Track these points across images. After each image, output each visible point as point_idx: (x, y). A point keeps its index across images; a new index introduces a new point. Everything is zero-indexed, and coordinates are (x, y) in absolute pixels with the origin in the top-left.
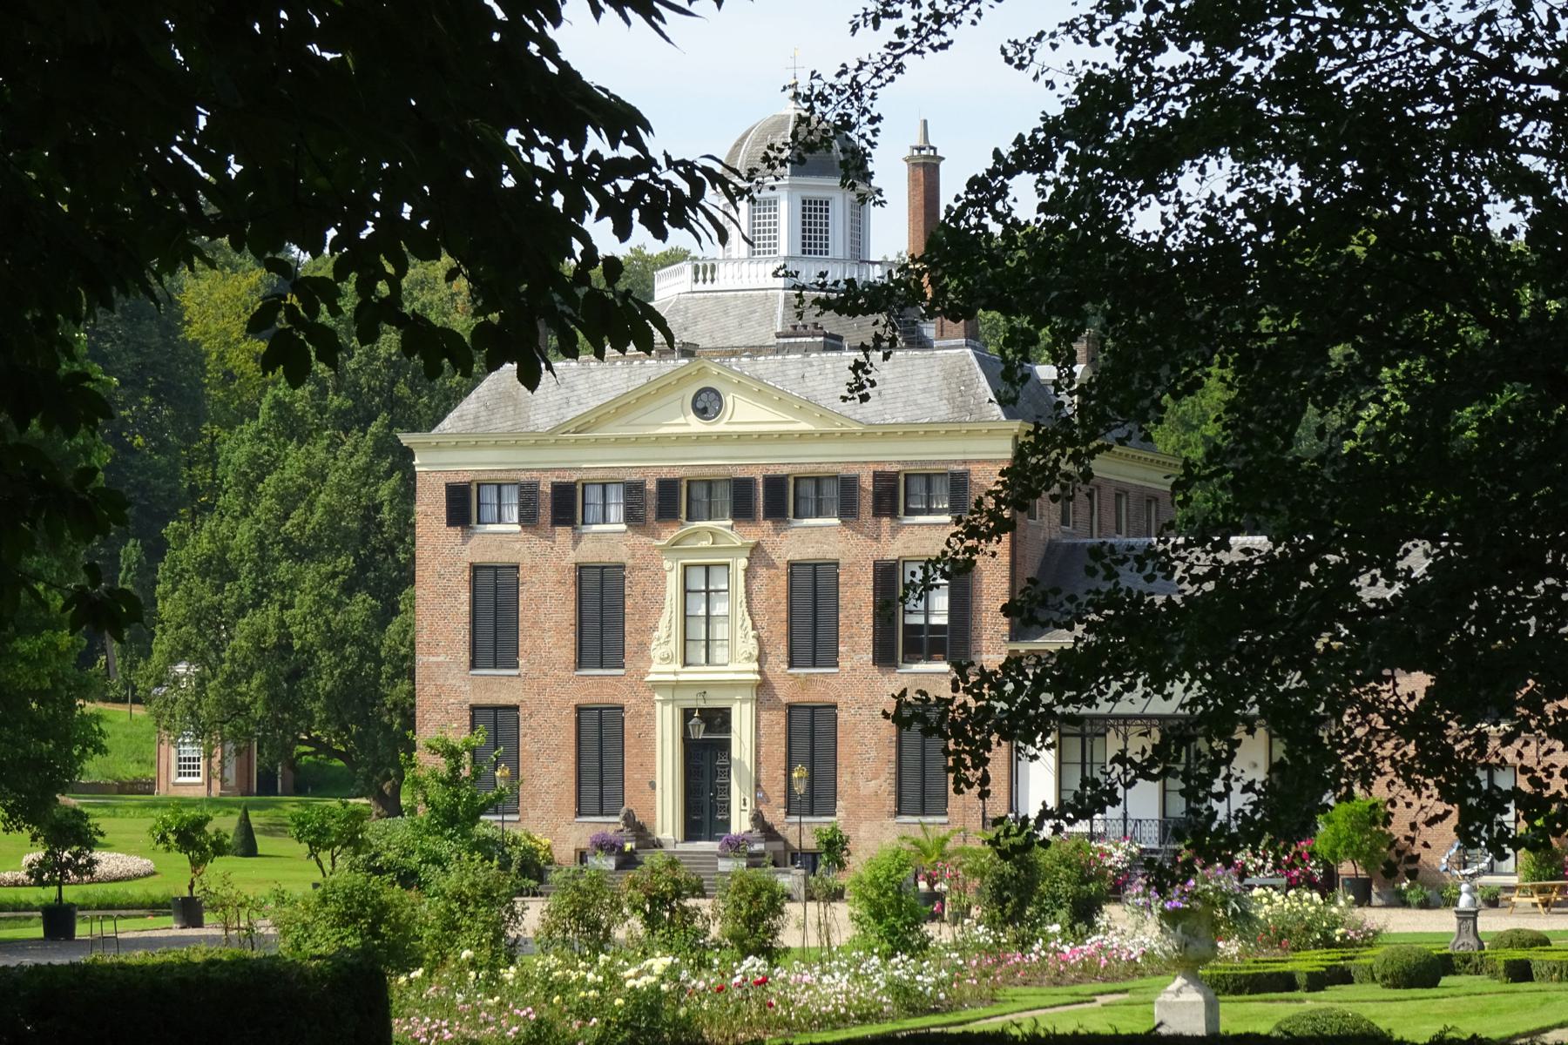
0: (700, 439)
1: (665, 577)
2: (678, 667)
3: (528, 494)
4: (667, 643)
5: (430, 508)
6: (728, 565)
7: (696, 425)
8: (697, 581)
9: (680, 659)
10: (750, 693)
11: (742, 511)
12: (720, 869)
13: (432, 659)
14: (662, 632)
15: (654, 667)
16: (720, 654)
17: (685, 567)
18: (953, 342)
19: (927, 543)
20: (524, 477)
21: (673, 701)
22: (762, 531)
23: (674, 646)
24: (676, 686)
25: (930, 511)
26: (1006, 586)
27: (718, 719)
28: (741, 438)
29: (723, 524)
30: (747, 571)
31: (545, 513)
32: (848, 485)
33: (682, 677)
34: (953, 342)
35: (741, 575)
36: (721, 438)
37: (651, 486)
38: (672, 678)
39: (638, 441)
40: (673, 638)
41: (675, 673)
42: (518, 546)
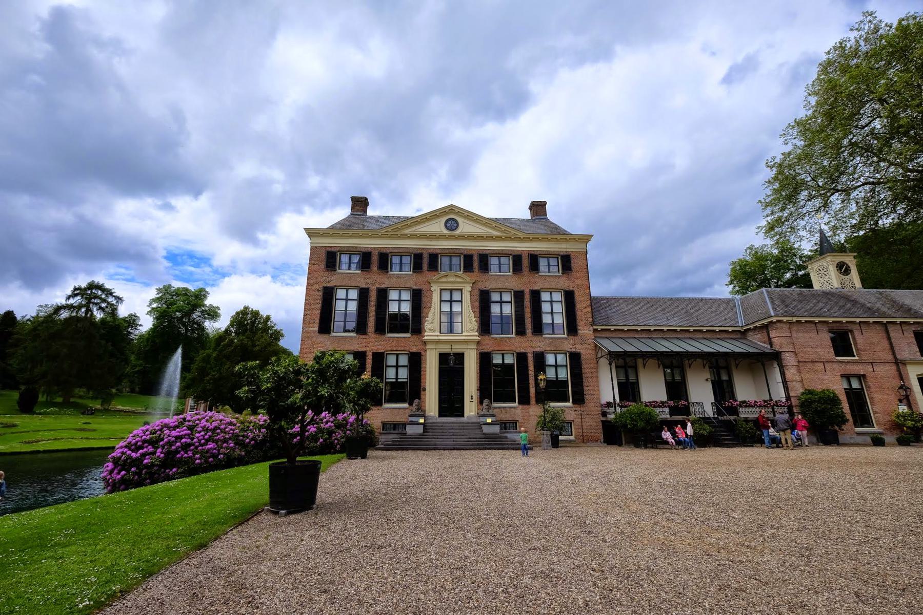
1: (431, 294)
2: (439, 334)
4: (432, 322)
6: (461, 290)
7: (446, 232)
8: (446, 296)
9: (438, 330)
11: (468, 266)
12: (484, 432)
13: (312, 329)
14: (429, 319)
15: (426, 334)
16: (457, 327)
17: (441, 290)
19: (553, 284)
20: (366, 250)
22: (476, 275)
23: (436, 325)
24: (438, 342)
25: (549, 272)
27: (460, 357)
33: (441, 338)
35: (468, 294)
36: (462, 237)
38: (436, 338)
41: (437, 336)
42: (359, 279)
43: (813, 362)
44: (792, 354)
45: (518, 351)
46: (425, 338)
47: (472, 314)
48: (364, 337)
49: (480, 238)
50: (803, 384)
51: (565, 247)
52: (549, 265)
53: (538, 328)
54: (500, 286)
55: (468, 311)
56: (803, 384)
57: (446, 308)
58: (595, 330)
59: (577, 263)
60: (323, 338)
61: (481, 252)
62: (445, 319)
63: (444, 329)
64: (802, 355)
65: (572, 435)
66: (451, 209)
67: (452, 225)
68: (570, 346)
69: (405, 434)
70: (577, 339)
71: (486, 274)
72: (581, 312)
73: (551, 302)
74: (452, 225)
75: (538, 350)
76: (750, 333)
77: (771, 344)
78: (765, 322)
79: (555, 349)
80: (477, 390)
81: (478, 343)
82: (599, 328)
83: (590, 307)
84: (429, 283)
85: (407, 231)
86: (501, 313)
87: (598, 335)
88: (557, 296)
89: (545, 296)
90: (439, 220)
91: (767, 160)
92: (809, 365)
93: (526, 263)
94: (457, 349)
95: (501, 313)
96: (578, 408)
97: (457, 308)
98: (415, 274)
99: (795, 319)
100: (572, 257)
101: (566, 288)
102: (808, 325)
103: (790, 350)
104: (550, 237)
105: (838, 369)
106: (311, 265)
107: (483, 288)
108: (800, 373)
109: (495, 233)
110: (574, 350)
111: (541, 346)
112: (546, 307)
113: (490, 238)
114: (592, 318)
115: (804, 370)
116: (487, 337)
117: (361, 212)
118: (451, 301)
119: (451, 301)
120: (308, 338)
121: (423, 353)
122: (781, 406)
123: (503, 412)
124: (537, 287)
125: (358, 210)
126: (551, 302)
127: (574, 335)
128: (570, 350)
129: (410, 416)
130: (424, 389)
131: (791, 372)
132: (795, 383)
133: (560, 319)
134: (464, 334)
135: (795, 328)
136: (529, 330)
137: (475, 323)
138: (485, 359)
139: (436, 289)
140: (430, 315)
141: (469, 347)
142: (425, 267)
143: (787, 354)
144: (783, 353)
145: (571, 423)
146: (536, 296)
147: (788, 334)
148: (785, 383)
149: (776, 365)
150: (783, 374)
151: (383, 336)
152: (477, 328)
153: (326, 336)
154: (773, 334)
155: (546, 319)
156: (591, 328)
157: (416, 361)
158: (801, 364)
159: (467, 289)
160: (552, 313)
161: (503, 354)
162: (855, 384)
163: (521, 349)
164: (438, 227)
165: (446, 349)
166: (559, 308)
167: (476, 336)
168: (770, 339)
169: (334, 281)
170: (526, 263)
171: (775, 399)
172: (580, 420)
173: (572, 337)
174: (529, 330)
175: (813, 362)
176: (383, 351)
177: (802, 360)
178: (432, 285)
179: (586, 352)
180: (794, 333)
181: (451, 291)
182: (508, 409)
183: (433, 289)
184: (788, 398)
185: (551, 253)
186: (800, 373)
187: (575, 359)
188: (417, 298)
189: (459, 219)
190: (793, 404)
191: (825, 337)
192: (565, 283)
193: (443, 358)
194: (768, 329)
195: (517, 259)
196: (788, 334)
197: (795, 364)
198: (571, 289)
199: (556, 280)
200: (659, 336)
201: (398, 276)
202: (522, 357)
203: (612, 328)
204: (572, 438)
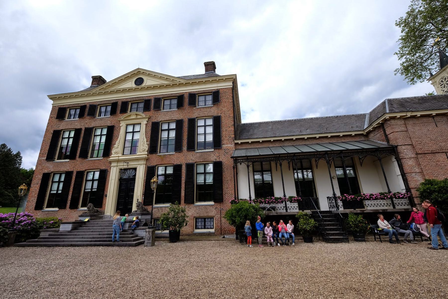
2: (120, 155)
4: (117, 148)
8: (130, 129)
10: (143, 162)
11: (147, 108)
15: (112, 156)
18: (210, 72)
19: (205, 113)
21: (117, 166)
22: (152, 113)
23: (120, 149)
24: (118, 161)
26: (233, 123)
30: (146, 124)
33: (120, 158)
34: (210, 72)
37: (120, 104)
40: (120, 147)
41: (119, 157)
43: (433, 153)
44: (409, 147)
45: (175, 163)
46: (111, 158)
47: (145, 140)
48: (74, 161)
50: (424, 175)
51: (216, 86)
52: (205, 101)
53: (192, 146)
54: (167, 118)
55: (142, 138)
56: (424, 175)
57: (129, 137)
58: (236, 144)
59: (225, 96)
61: (157, 97)
62: (128, 145)
63: (127, 151)
64: (421, 147)
65: (213, 228)
66: (138, 71)
67: (139, 81)
68: (215, 157)
69: (58, 231)
70: (221, 152)
71: (159, 111)
72: (226, 131)
73: (205, 126)
74: (139, 81)
75: (191, 162)
76: (372, 135)
77: (388, 140)
78: (380, 121)
79: (203, 160)
80: (143, 194)
82: (239, 142)
83: (233, 127)
84: (119, 121)
86: (168, 137)
87: (239, 147)
88: (210, 122)
89: (201, 123)
90: (131, 80)
91: (396, 21)
92: (429, 157)
93: (186, 100)
94: (132, 165)
95: (168, 137)
96: (218, 206)
97: (137, 136)
98: (112, 117)
99: (409, 114)
100: (221, 91)
101: (215, 114)
102: (425, 119)
103: (406, 144)
104: (204, 80)
106: (51, 117)
108: (419, 165)
110: (218, 160)
111: (193, 159)
112: (201, 130)
113: (161, 87)
114: (235, 134)
115: (423, 161)
116: (154, 155)
117: (96, 85)
118: (133, 132)
120: (40, 164)
121: (109, 170)
122: (399, 198)
123: (160, 211)
124: (194, 116)
125: (95, 84)
127: (219, 149)
128: (215, 160)
129: (80, 216)
130: (106, 196)
131: (409, 164)
132: (414, 174)
133: (210, 138)
134: (138, 154)
135: (411, 122)
136: (185, 148)
137: (147, 146)
139: (123, 125)
140: (117, 143)
141: (140, 163)
143: (403, 147)
144: (399, 147)
145: (213, 218)
146: (192, 123)
147: (404, 129)
148: (403, 175)
149: (394, 159)
150: (401, 167)
151: (85, 160)
152: (147, 149)
153: (51, 162)
154: (388, 131)
155: (201, 139)
156: (233, 143)
157: (104, 175)
158: (419, 156)
159: (144, 122)
160: (205, 134)
161: (166, 167)
163: (177, 162)
164: (131, 84)
165: (124, 166)
166: (210, 130)
167: (145, 155)
168: (386, 136)
169: (61, 126)
170: (186, 100)
171: (393, 191)
172: (219, 216)
173: (218, 150)
174: (185, 148)
175: (433, 153)
176: (84, 170)
177: (420, 152)
178: (121, 122)
179: (227, 162)
180: (410, 128)
181: (134, 125)
182: (164, 209)
183: (121, 125)
184: (408, 189)
185: (206, 92)
186: (419, 165)
187: (218, 166)
189: (144, 78)
190: (414, 196)
192: (215, 111)
193: (123, 171)
194: (384, 127)
195: (180, 99)
196: (404, 129)
197: (413, 156)
198: (219, 115)
199: (208, 110)
200: (290, 144)
201: (101, 119)
202: (177, 168)
203: (250, 141)
204: (213, 231)
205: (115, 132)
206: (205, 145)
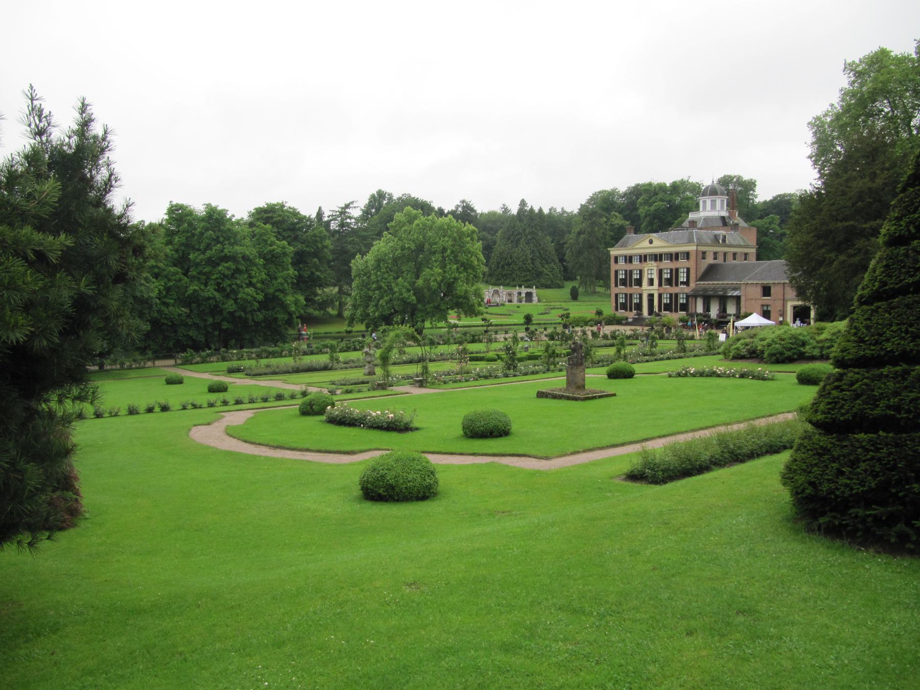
0: (650, 248)
3: (640, 256)
5: (612, 260)
10: (657, 291)
11: (656, 260)
24: (646, 290)
28: (655, 247)
29: (653, 262)
31: (628, 261)
32: (671, 254)
36: (653, 248)
39: (641, 248)
43: (752, 299)
49: (658, 247)
60: (616, 288)
67: (651, 242)
70: (690, 288)
74: (651, 242)
81: (658, 290)
85: (637, 246)
88: (685, 270)
94: (652, 292)
105: (760, 302)
107: (660, 268)
109: (666, 245)
112: (682, 275)
118: (651, 274)
119: (651, 274)
124: (677, 267)
126: (684, 272)
136: (674, 285)
138: (660, 296)
139: (646, 269)
142: (643, 261)
146: (677, 270)
157: (641, 295)
162: (769, 309)
174: (674, 285)
175: (752, 299)
181: (651, 270)
188: (641, 271)
191: (759, 290)
205: (643, 274)
206: (682, 283)
